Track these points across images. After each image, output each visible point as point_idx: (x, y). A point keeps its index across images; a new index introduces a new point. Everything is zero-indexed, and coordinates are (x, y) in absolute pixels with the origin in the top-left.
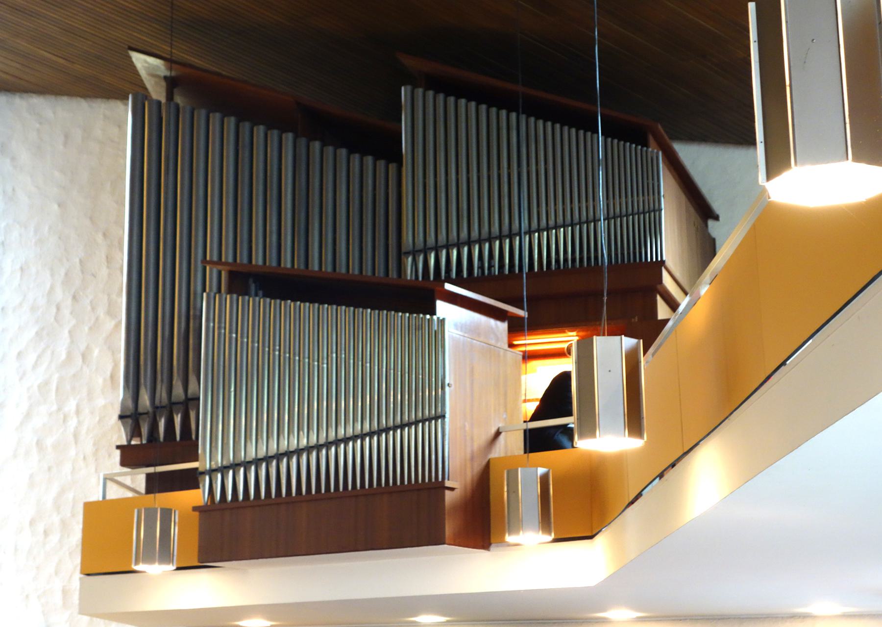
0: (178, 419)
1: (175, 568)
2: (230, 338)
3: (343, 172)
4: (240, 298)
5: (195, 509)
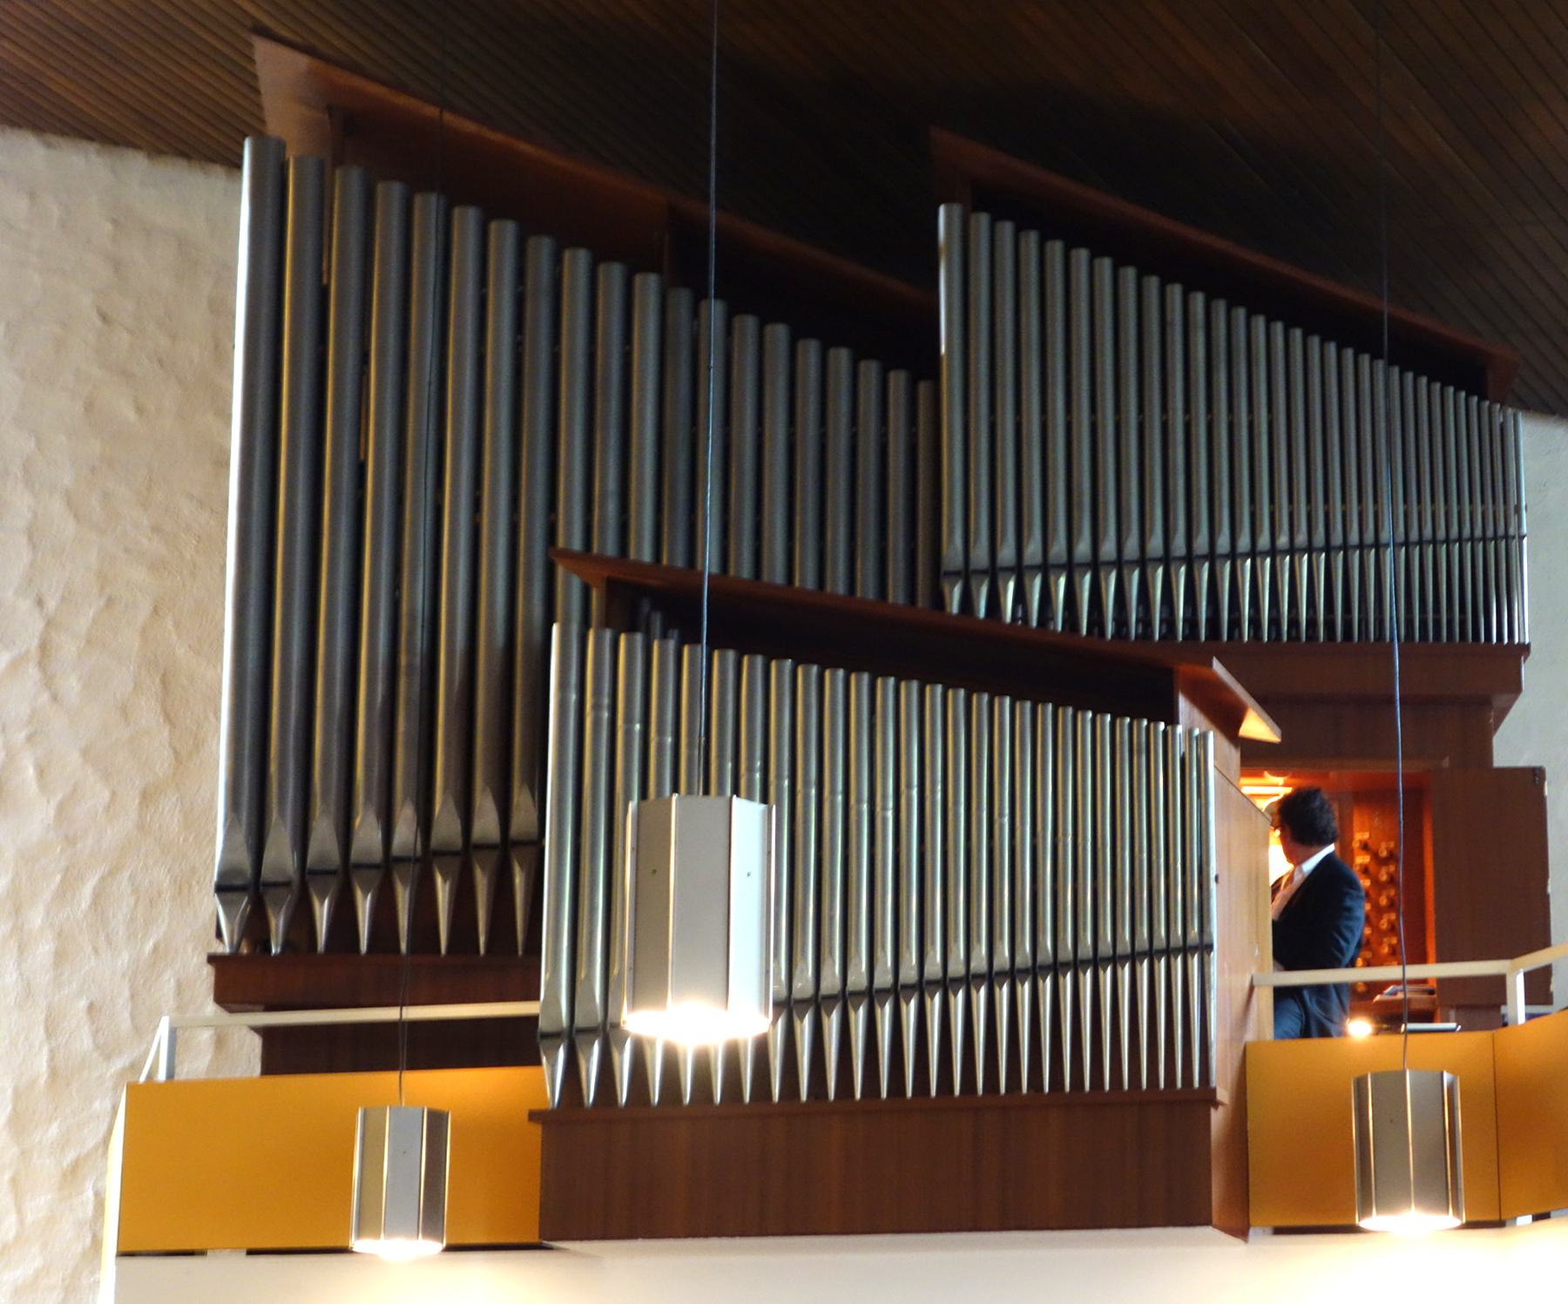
0: (364, 906)
1: (1458, 1222)
2: (629, 732)
3: (770, 377)
4: (623, 638)
5: (534, 1116)
